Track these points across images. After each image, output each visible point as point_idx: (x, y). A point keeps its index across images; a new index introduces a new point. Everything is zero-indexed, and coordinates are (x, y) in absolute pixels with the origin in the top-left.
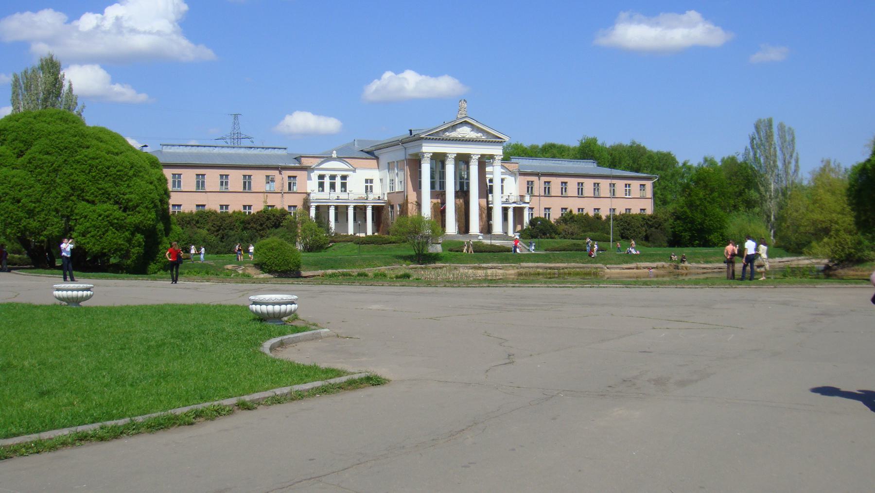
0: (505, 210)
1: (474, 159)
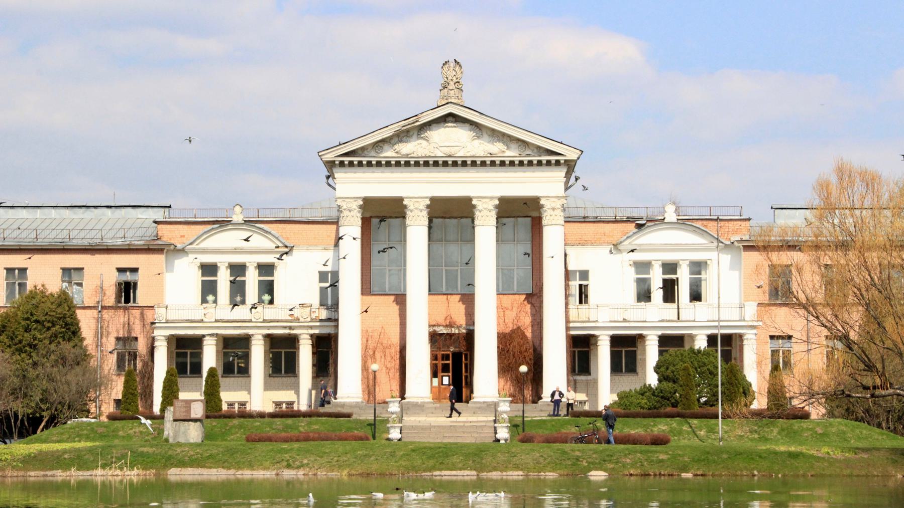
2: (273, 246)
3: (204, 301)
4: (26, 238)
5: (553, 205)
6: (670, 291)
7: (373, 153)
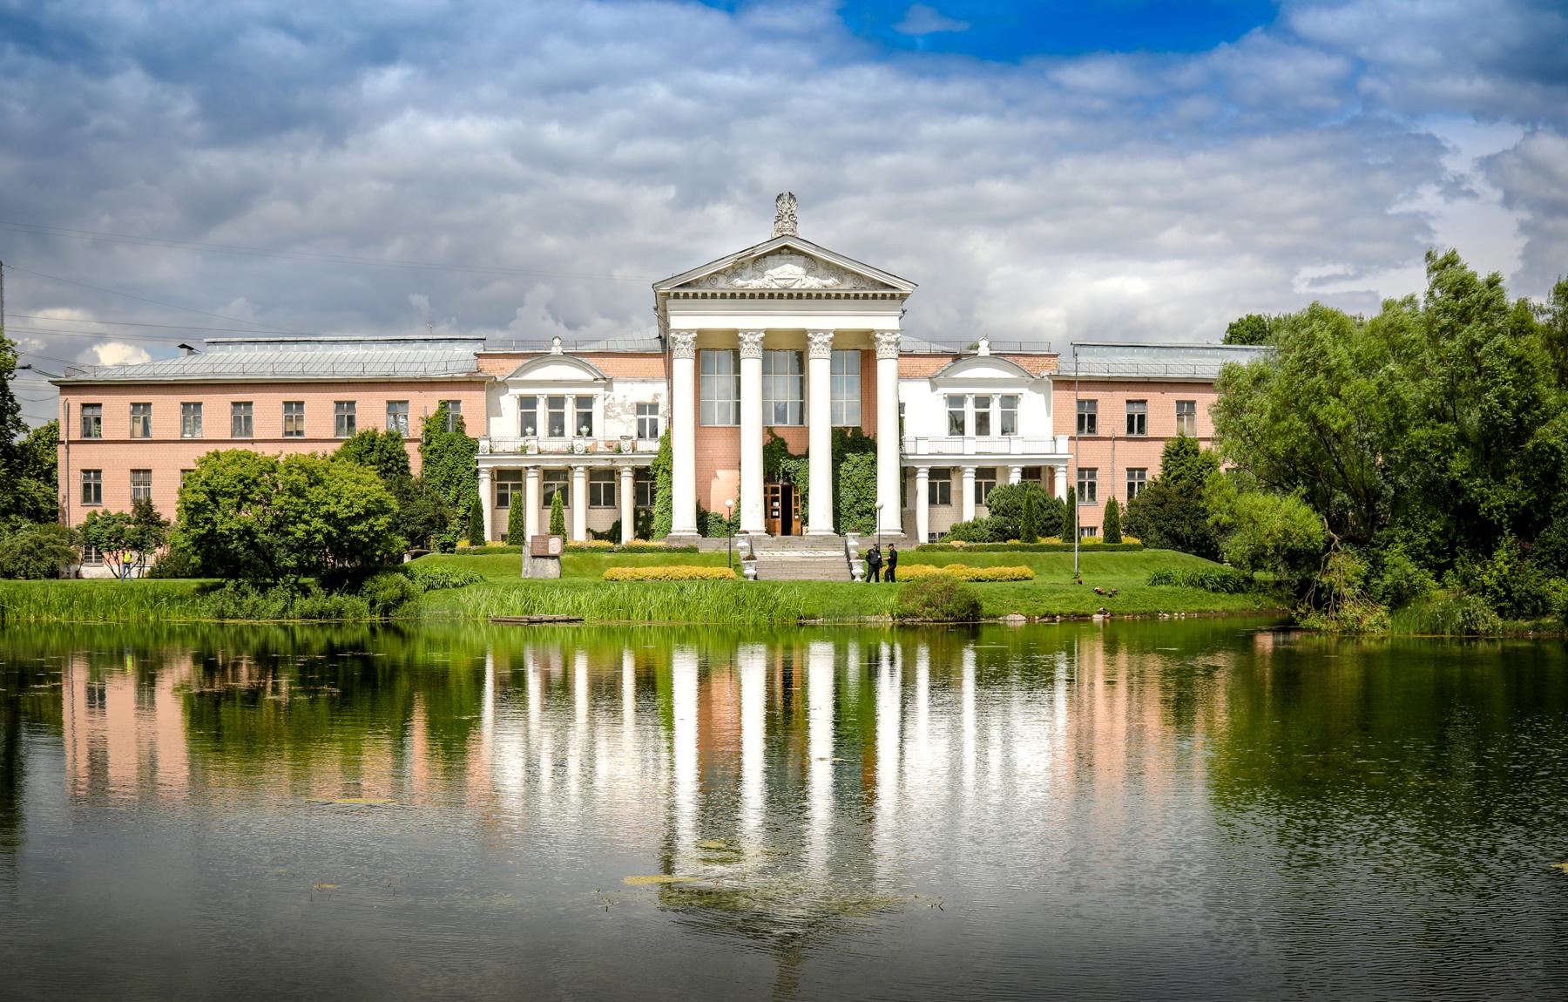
0: (907, 475)
1: (816, 344)
2: (592, 378)
3: (524, 434)
4: (354, 373)
5: (889, 338)
6: (983, 423)
7: (708, 285)
